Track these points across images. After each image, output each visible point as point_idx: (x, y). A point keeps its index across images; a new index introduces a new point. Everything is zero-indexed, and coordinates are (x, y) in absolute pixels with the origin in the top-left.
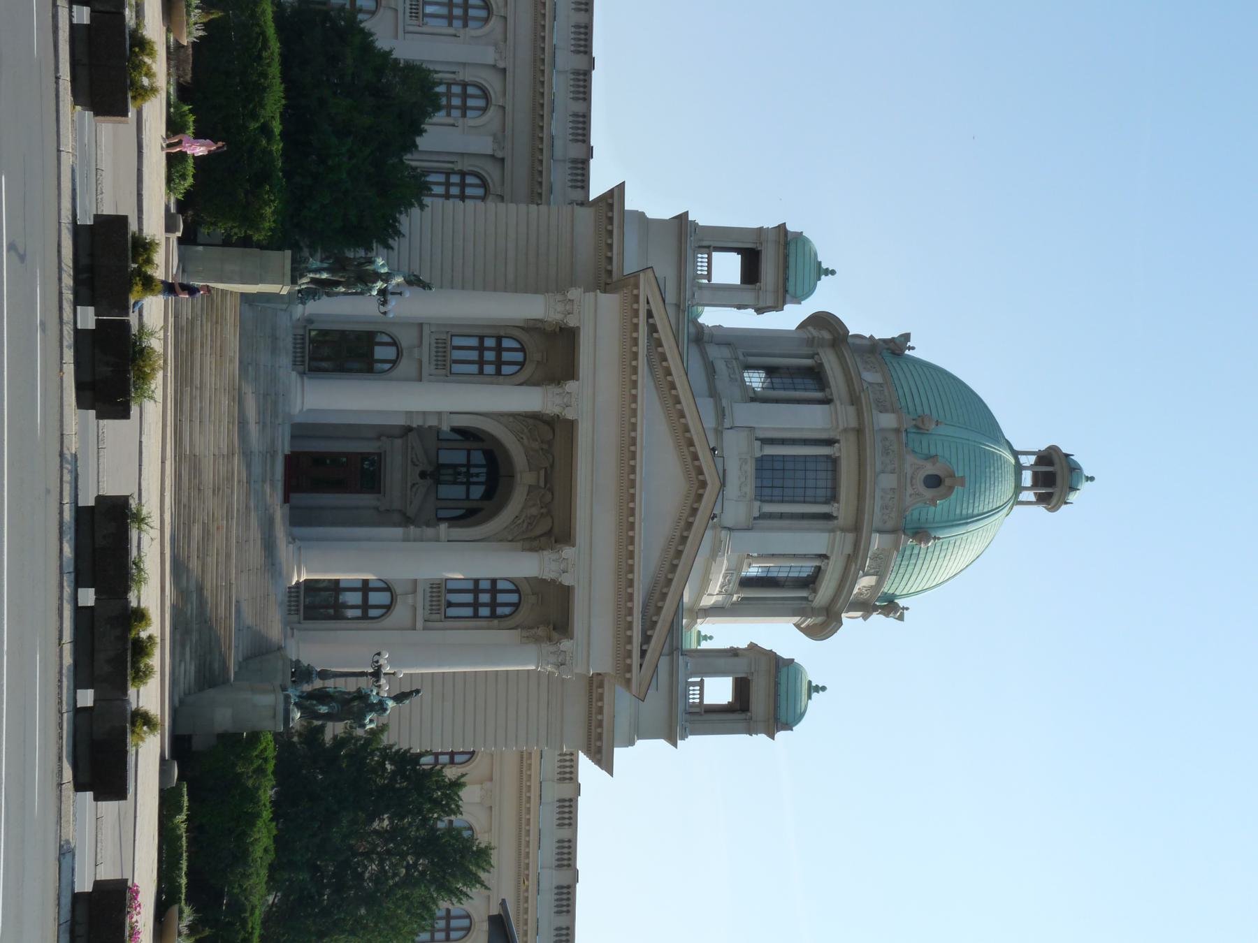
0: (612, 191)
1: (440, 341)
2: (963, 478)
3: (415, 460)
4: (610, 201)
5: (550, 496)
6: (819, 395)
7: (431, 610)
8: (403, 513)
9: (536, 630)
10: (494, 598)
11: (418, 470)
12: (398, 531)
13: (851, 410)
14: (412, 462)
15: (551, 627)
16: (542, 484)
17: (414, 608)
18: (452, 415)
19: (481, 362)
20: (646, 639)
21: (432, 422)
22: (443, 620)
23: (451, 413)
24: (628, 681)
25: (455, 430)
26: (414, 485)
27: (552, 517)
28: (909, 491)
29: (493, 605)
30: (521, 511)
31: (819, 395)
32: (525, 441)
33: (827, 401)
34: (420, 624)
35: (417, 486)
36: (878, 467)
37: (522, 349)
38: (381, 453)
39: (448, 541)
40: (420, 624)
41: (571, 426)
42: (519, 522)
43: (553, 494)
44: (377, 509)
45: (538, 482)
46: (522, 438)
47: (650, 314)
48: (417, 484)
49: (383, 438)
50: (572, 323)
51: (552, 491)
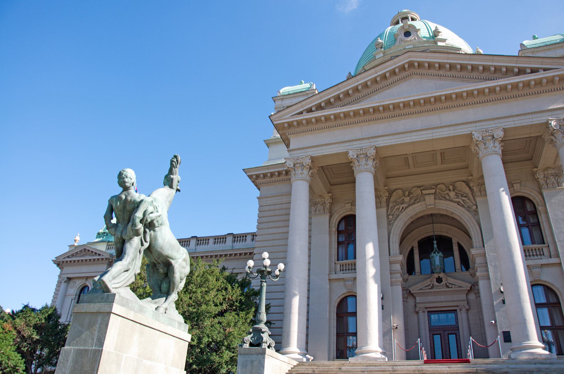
0: (250, 177)
1: (342, 269)
3: (430, 287)
4: (254, 177)
5: (439, 185)
7: (540, 255)
8: (469, 291)
9: (540, 180)
11: (436, 283)
14: (431, 288)
15: (535, 170)
16: (433, 191)
17: (542, 266)
21: (398, 267)
22: (546, 245)
23: (390, 255)
26: (448, 287)
27: (455, 182)
30: (454, 202)
32: (404, 205)
34: (554, 260)
35: (448, 284)
38: (428, 312)
39: (484, 246)
40: (554, 260)
42: (462, 202)
43: (439, 184)
44: (468, 310)
45: (432, 194)
46: (403, 208)
47: (301, 113)
48: (446, 284)
49: (417, 309)
50: (308, 161)
51: (436, 185)
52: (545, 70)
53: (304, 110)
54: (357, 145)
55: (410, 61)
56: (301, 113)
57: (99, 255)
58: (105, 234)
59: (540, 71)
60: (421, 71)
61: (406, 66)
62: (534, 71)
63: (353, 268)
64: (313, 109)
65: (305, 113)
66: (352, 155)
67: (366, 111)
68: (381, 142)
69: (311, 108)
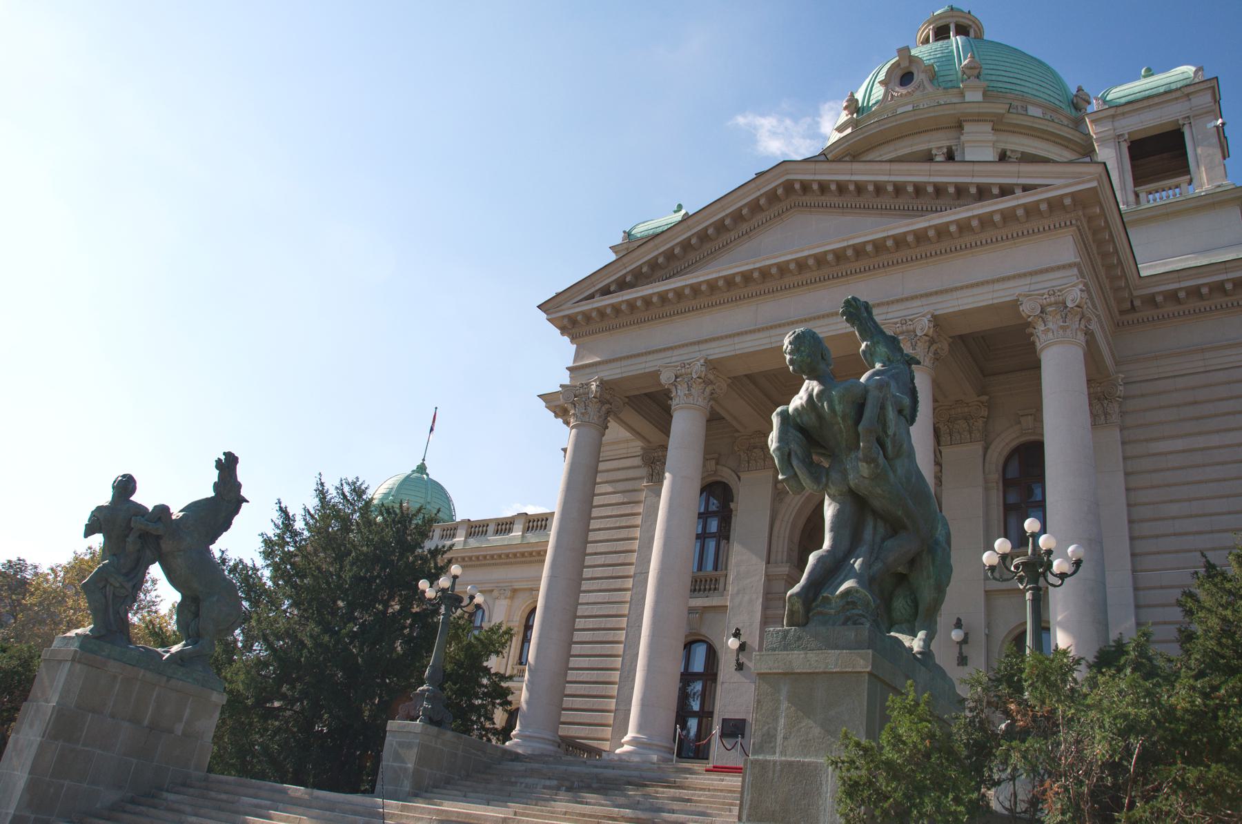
18: (772, 560)
23: (768, 562)
52: (1026, 188)
53: (596, 291)
54: (676, 357)
55: (787, 180)
56: (591, 297)
59: (1016, 191)
60: (807, 199)
61: (780, 191)
62: (1006, 191)
63: (712, 586)
64: (612, 288)
65: (597, 298)
66: (666, 378)
67: (712, 286)
68: (717, 351)
69: (608, 286)
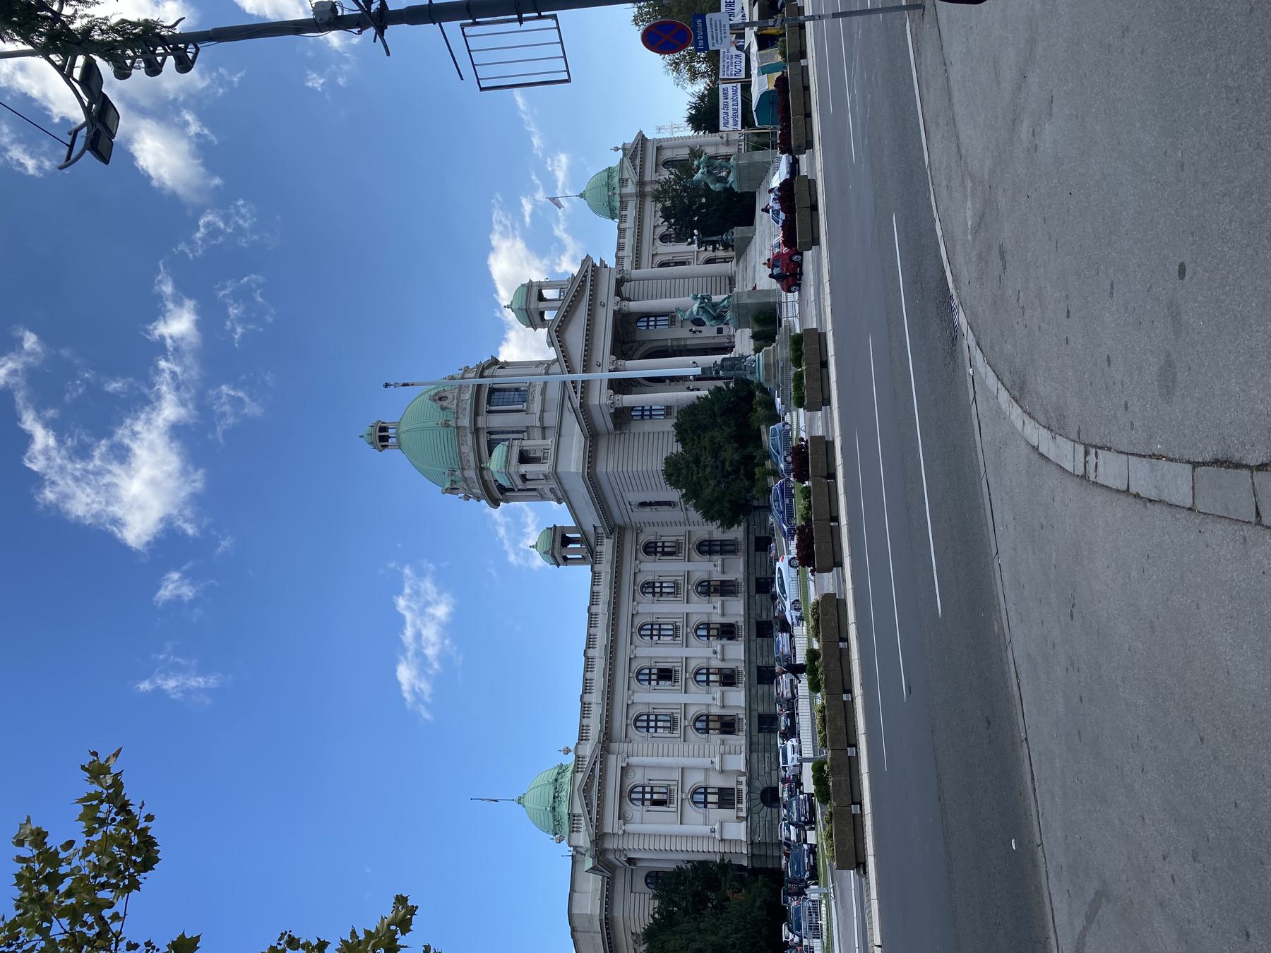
2: (430, 399)
6: (493, 437)
10: (648, 324)
12: (689, 342)
13: (479, 425)
19: (651, 410)
20: (585, 276)
24: (593, 267)
25: (664, 381)
28: (455, 394)
29: (648, 326)
31: (493, 437)
33: (490, 433)
36: (469, 401)
37: (632, 416)
41: (613, 353)
57: (594, 764)
58: (556, 794)
